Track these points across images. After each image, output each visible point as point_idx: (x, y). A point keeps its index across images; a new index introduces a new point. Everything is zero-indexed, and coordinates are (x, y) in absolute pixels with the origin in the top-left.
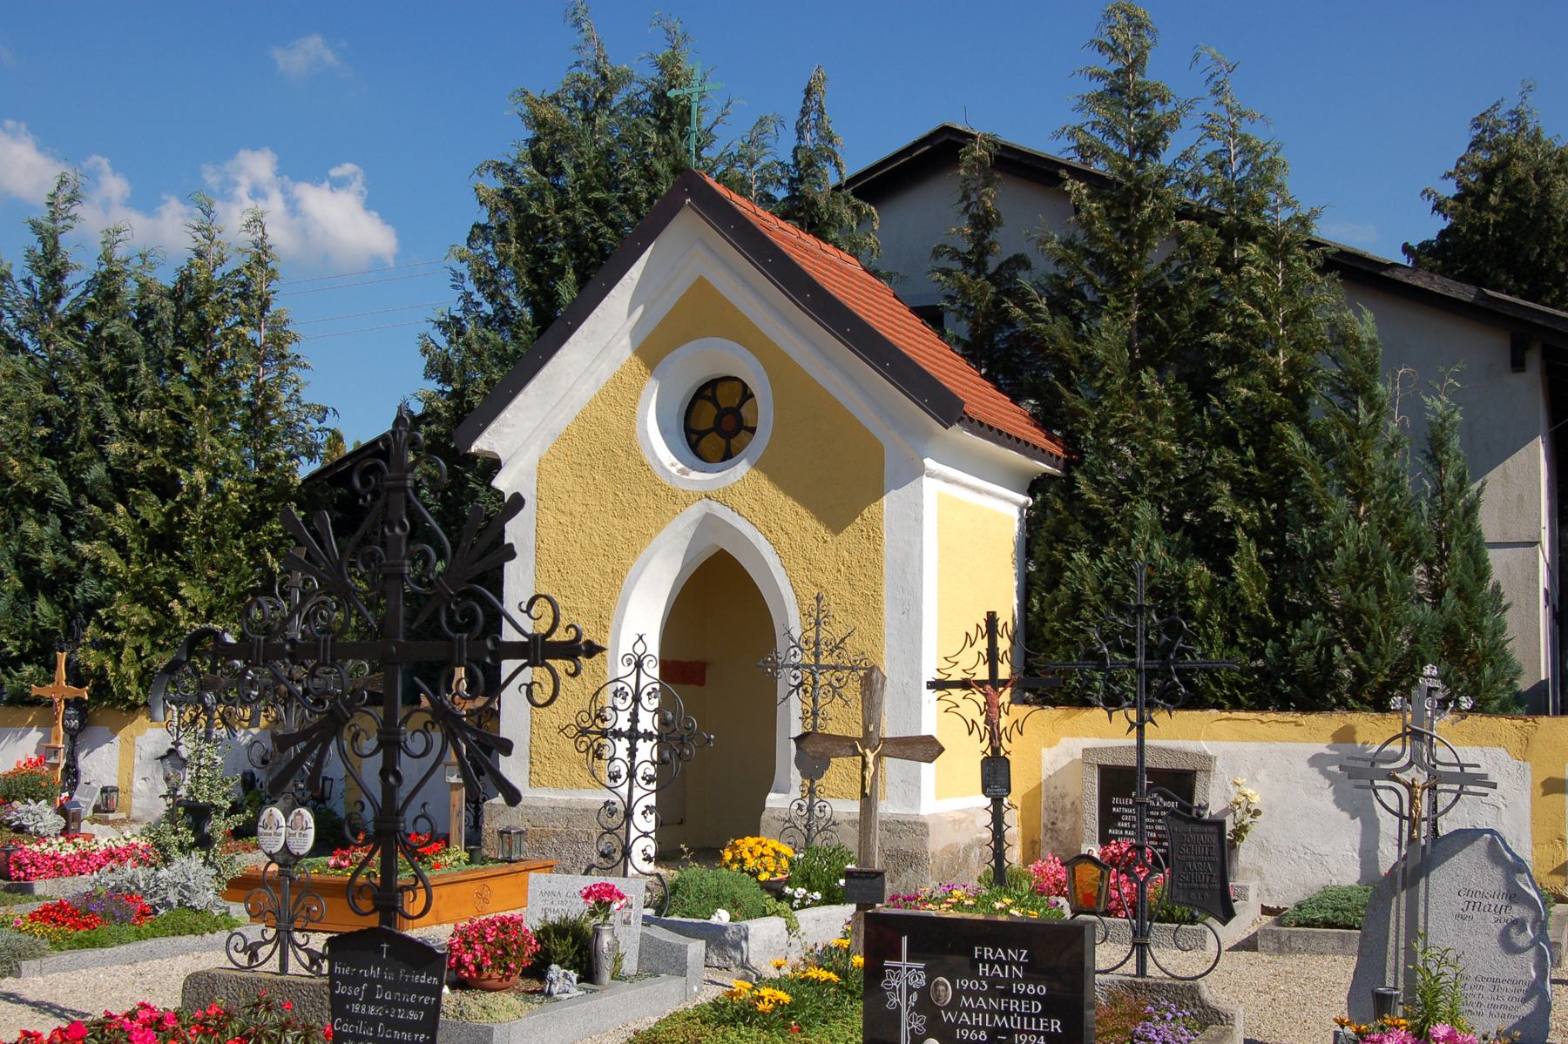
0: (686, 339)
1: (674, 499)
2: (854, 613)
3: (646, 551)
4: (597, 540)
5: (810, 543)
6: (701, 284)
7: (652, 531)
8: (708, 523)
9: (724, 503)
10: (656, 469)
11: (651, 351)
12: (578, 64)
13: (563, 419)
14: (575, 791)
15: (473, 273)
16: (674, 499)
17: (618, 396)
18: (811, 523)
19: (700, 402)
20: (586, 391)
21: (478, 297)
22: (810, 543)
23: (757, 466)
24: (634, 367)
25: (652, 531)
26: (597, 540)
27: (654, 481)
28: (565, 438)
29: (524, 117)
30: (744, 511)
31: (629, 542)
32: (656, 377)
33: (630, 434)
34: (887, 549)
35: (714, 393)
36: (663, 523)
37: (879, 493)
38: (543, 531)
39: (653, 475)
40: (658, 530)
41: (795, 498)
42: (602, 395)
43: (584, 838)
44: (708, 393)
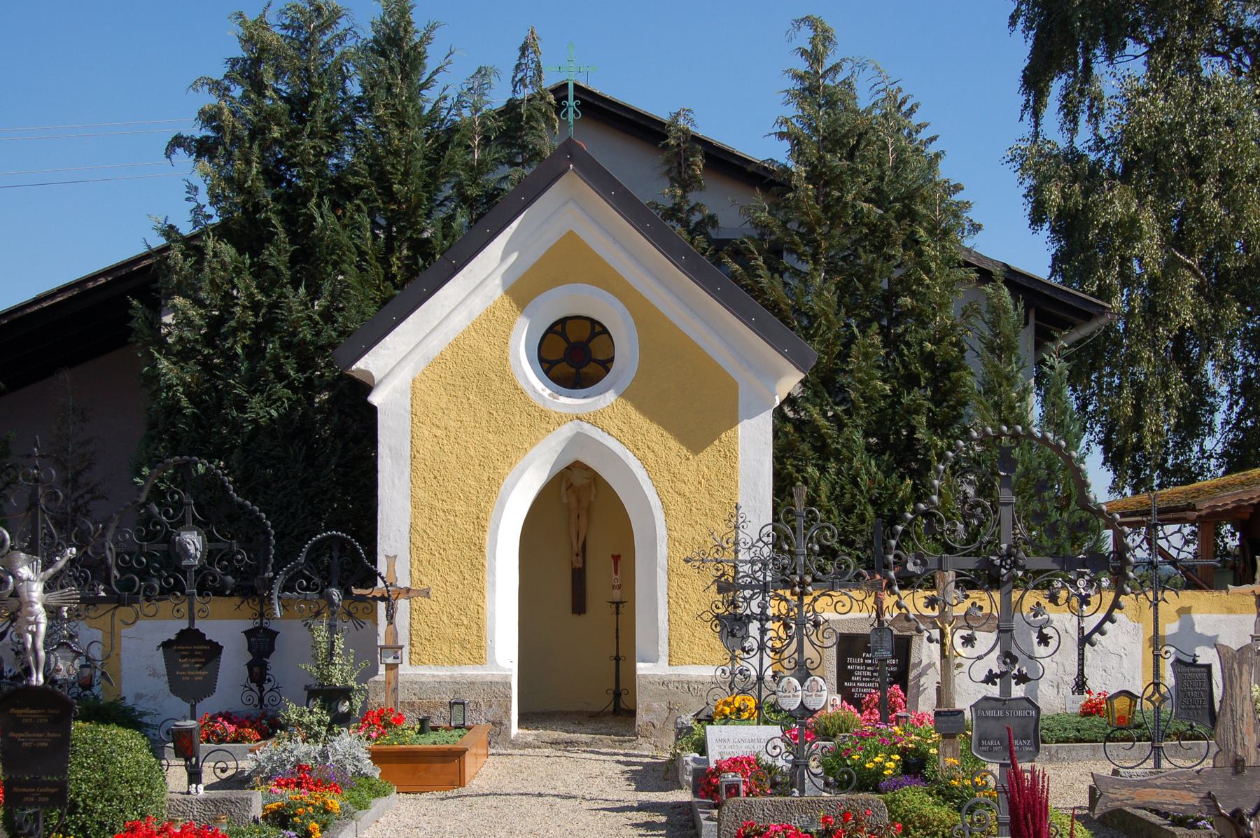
1: (549, 420)
3: (521, 463)
4: (472, 452)
8: (579, 439)
9: (595, 424)
11: (521, 292)
13: (437, 345)
14: (456, 667)
16: (549, 420)
17: (491, 326)
18: (673, 443)
20: (460, 322)
24: (507, 304)
26: (472, 452)
27: (528, 402)
28: (439, 361)
30: (614, 431)
31: (505, 455)
32: (529, 317)
33: (503, 360)
36: (537, 439)
38: (417, 442)
39: (527, 398)
40: (532, 445)
41: (660, 423)
42: (476, 326)
44: (558, 328)
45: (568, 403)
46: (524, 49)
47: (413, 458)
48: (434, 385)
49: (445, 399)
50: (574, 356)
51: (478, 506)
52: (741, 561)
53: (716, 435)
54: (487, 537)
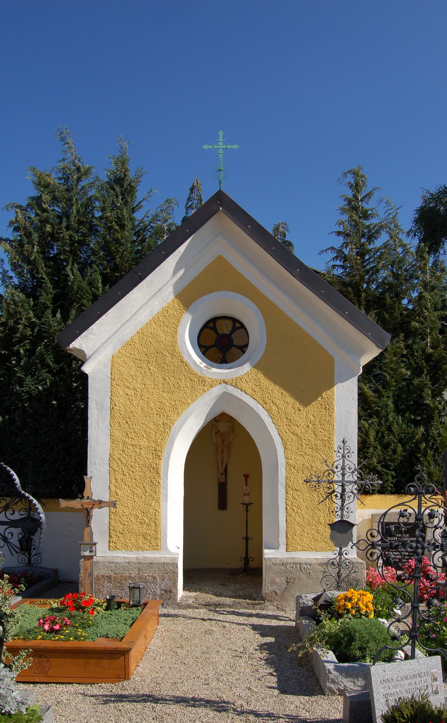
0: (210, 291)
1: (204, 383)
2: (317, 450)
3: (185, 413)
4: (152, 405)
5: (290, 411)
6: (220, 259)
7: (189, 401)
8: (225, 397)
9: (236, 386)
10: (192, 365)
11: (187, 296)
12: (64, 160)
13: (129, 332)
14: (140, 552)
15: (11, 260)
16: (204, 383)
17: (165, 320)
18: (290, 400)
19: (206, 330)
20: (144, 317)
21: (11, 274)
22: (290, 411)
23: (256, 366)
24: (176, 305)
25: (189, 401)
26: (152, 405)
27: (191, 372)
28: (130, 344)
29: (34, 183)
30: (249, 391)
31: (174, 407)
32: (191, 313)
33: (174, 344)
34: (336, 415)
35: (215, 325)
36: (196, 396)
37: (331, 385)
38: (115, 399)
39: (189, 368)
40: (193, 400)
41: (281, 386)
42: (155, 320)
43: (151, 579)
44: (211, 325)
45: (217, 372)
46: (192, 190)
47: (112, 409)
48: (127, 360)
49: (134, 369)
50: (221, 341)
51: (156, 442)
52: (348, 482)
53: (319, 394)
54: (162, 463)
